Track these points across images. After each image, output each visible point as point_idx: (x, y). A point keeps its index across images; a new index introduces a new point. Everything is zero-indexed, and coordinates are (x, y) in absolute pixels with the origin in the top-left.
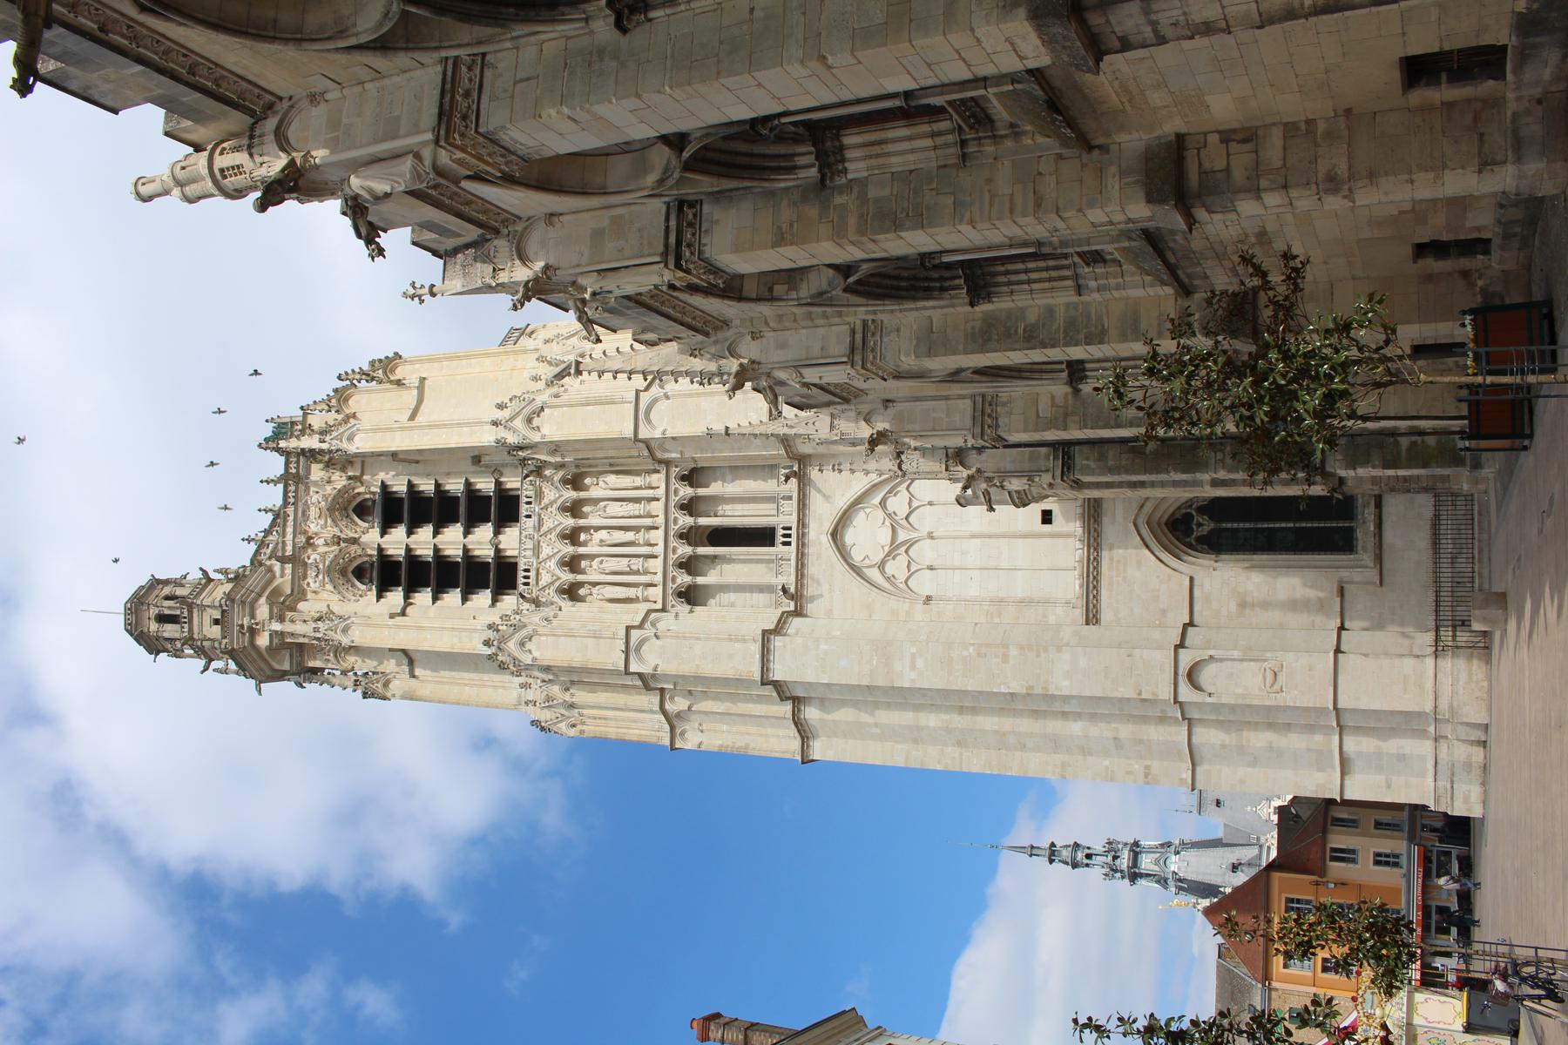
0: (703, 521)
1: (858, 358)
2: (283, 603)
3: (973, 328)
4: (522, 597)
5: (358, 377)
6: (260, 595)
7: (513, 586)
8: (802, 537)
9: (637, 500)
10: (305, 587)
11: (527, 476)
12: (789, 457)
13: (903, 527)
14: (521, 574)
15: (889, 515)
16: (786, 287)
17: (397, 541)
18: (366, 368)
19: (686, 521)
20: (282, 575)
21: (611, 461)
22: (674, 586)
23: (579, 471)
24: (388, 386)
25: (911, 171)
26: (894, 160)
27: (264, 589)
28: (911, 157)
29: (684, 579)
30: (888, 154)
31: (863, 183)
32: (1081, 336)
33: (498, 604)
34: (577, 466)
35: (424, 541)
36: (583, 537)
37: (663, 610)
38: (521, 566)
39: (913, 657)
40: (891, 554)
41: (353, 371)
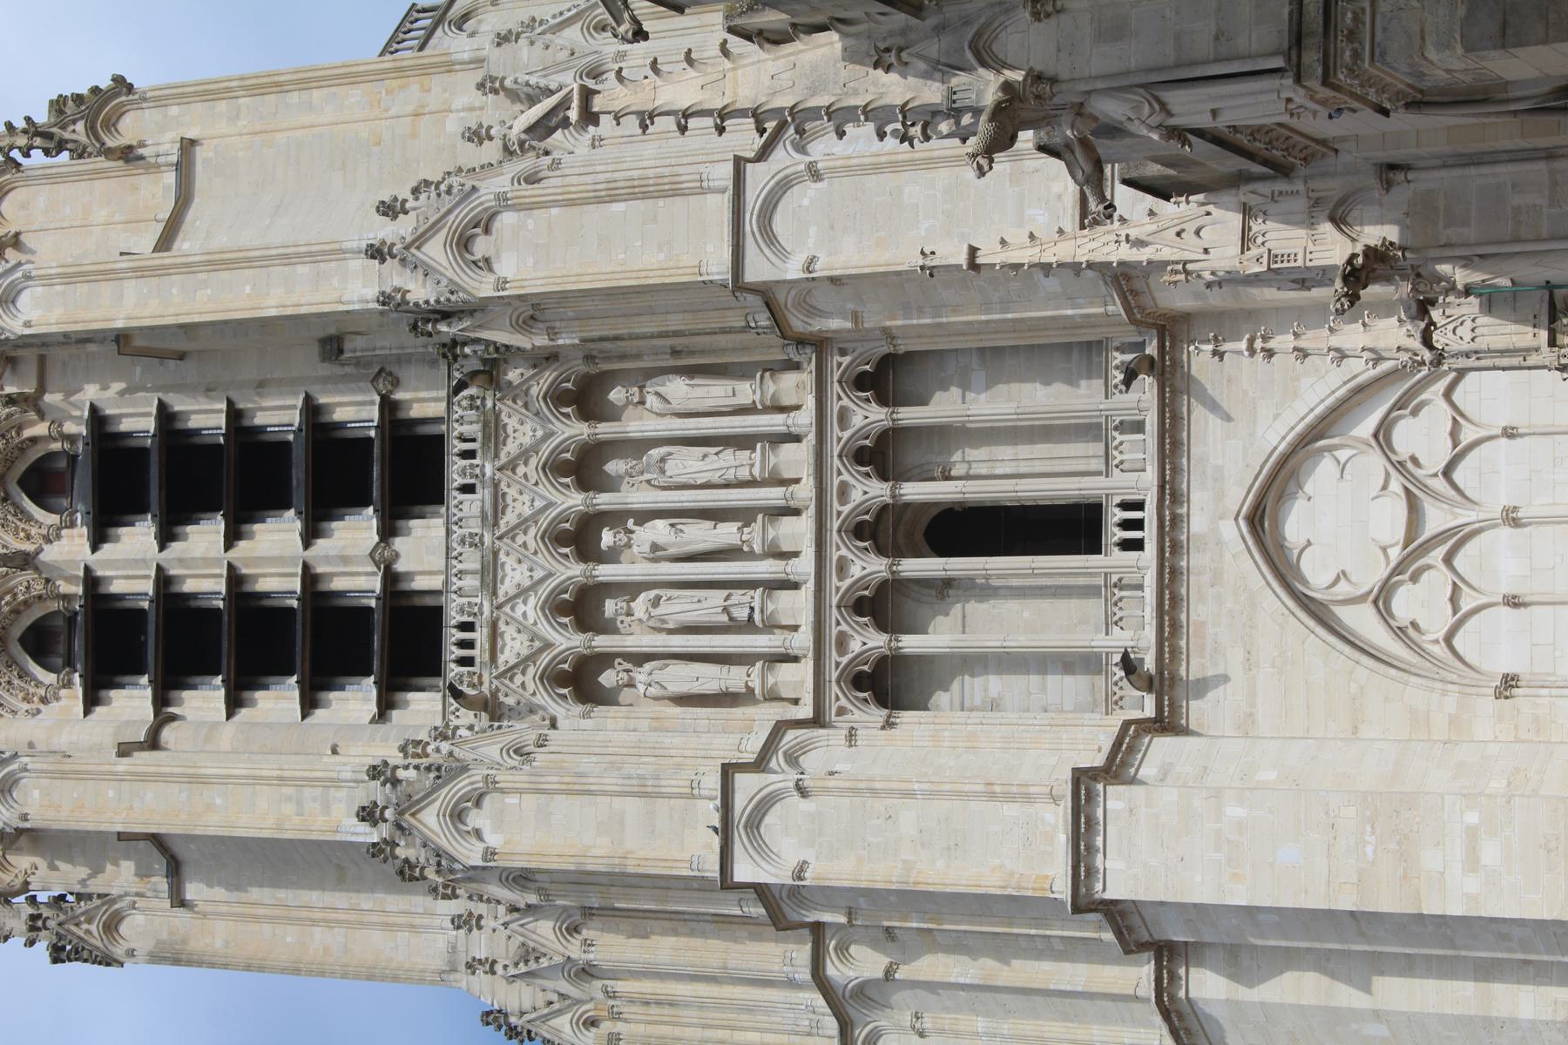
0: (914, 491)
1: (1312, 58)
4: (457, 694)
5: (22, 141)
9: (743, 442)
11: (462, 386)
12: (1133, 321)
13: (1436, 496)
14: (452, 635)
15: (1400, 466)
18: (42, 117)
19: (869, 491)
21: (677, 342)
22: (845, 660)
23: (593, 370)
24: (101, 163)
29: (868, 641)
33: (395, 714)
34: (589, 358)
36: (607, 538)
37: (818, 721)
38: (453, 616)
39: (1472, 834)
40: (1408, 566)
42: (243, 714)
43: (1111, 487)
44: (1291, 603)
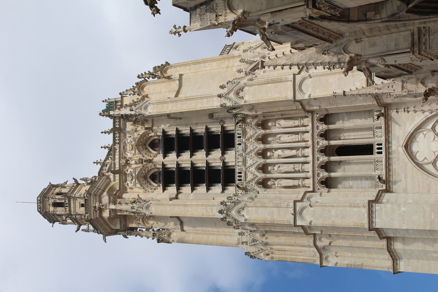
0: (333, 143)
1: (416, 49)
2: (115, 194)
4: (238, 187)
5: (148, 76)
6: (103, 191)
7: (234, 182)
8: (388, 149)
10: (126, 186)
11: (238, 123)
12: (379, 105)
14: (237, 175)
16: (374, 13)
18: (152, 71)
19: (323, 143)
22: (319, 178)
23: (265, 119)
24: (164, 80)
27: (105, 188)
29: (324, 174)
33: (226, 191)
36: (269, 154)
37: (313, 191)
38: (237, 171)
41: (145, 73)
42: (195, 191)
44: (414, 164)
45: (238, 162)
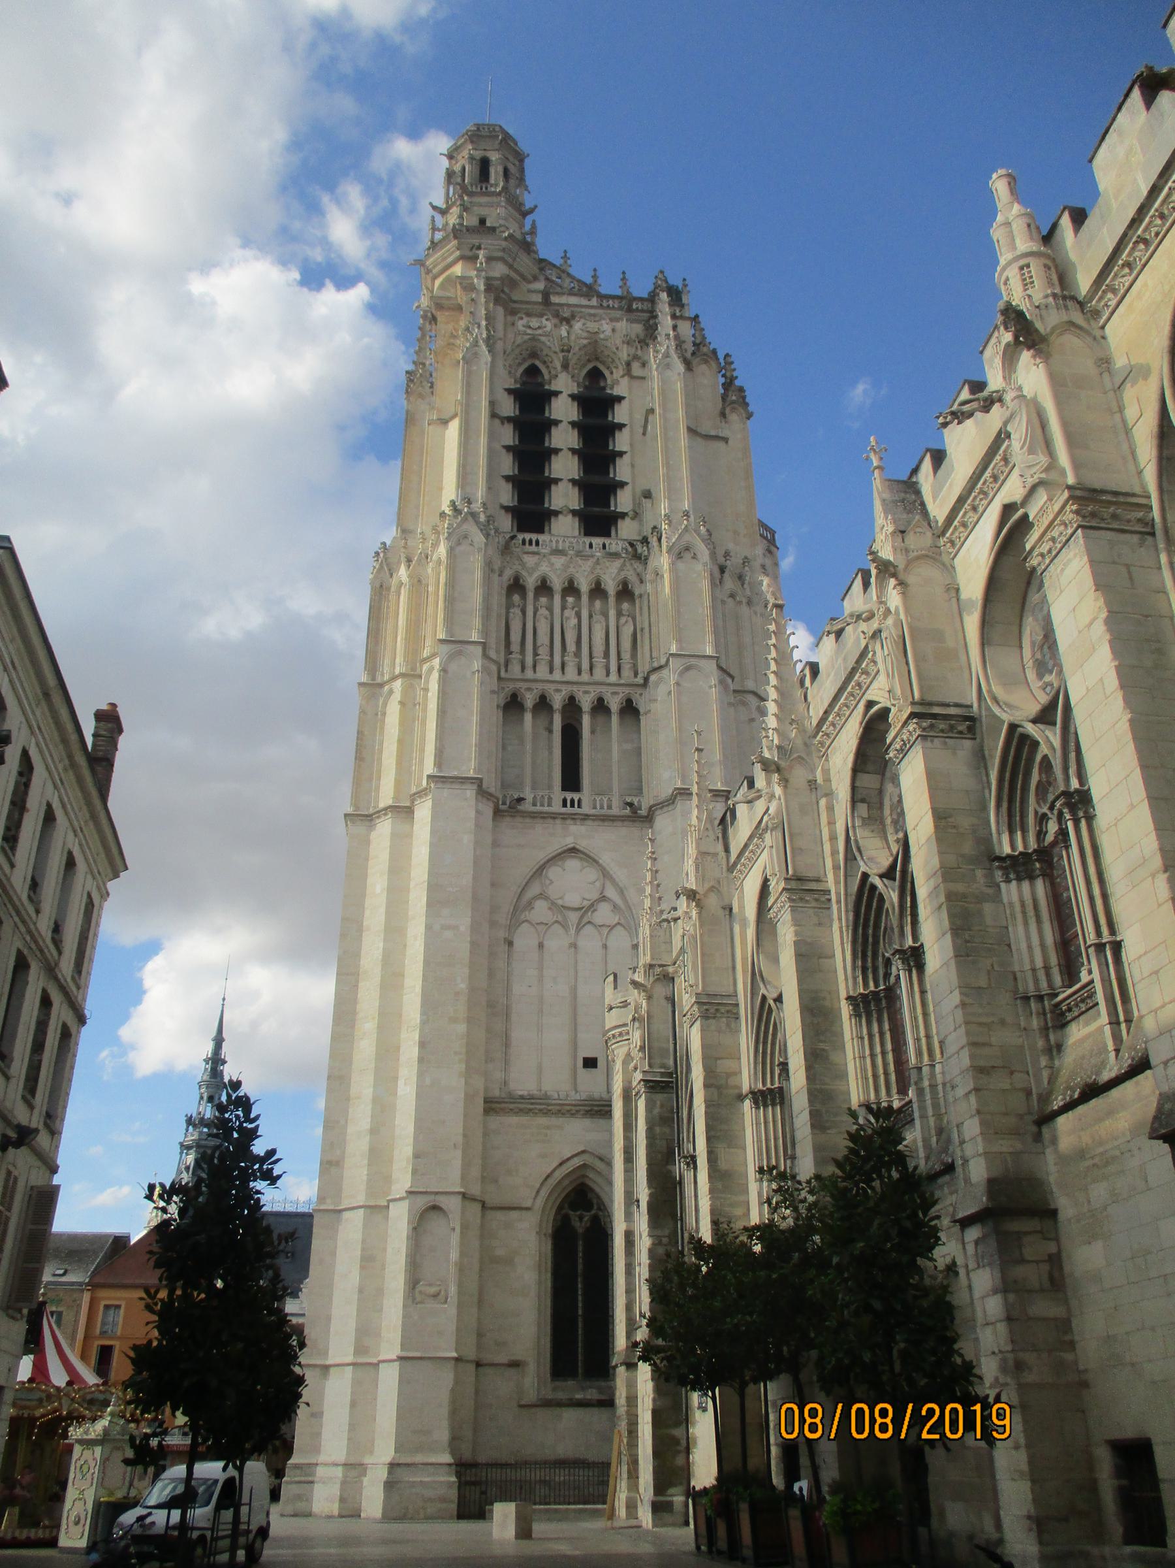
0: (586, 720)
1: (793, 885)
2: (503, 291)
3: (824, 999)
4: (513, 537)
5: (728, 374)
6: (511, 267)
7: (522, 528)
8: (573, 817)
9: (607, 654)
10: (519, 315)
11: (632, 545)
12: (651, 807)
13: (582, 917)
14: (534, 537)
15: (592, 905)
16: (866, 815)
17: (563, 410)
18: (737, 383)
19: (586, 703)
20: (530, 291)
21: (647, 630)
22: (522, 690)
23: (636, 597)
24: (720, 405)
25: (1009, 946)
26: (1021, 929)
27: (516, 271)
28: (1024, 946)
29: (529, 700)
30: (1026, 923)
31: (997, 898)
32: (818, 1106)
33: (503, 512)
34: (641, 596)
35: (564, 438)
36: (570, 600)
37: (499, 678)
38: (541, 538)
39: (455, 928)
40: (553, 906)
41: (734, 370)
42: (504, 451)
43: (586, 795)
44: (542, 862)
45: (557, 542)
